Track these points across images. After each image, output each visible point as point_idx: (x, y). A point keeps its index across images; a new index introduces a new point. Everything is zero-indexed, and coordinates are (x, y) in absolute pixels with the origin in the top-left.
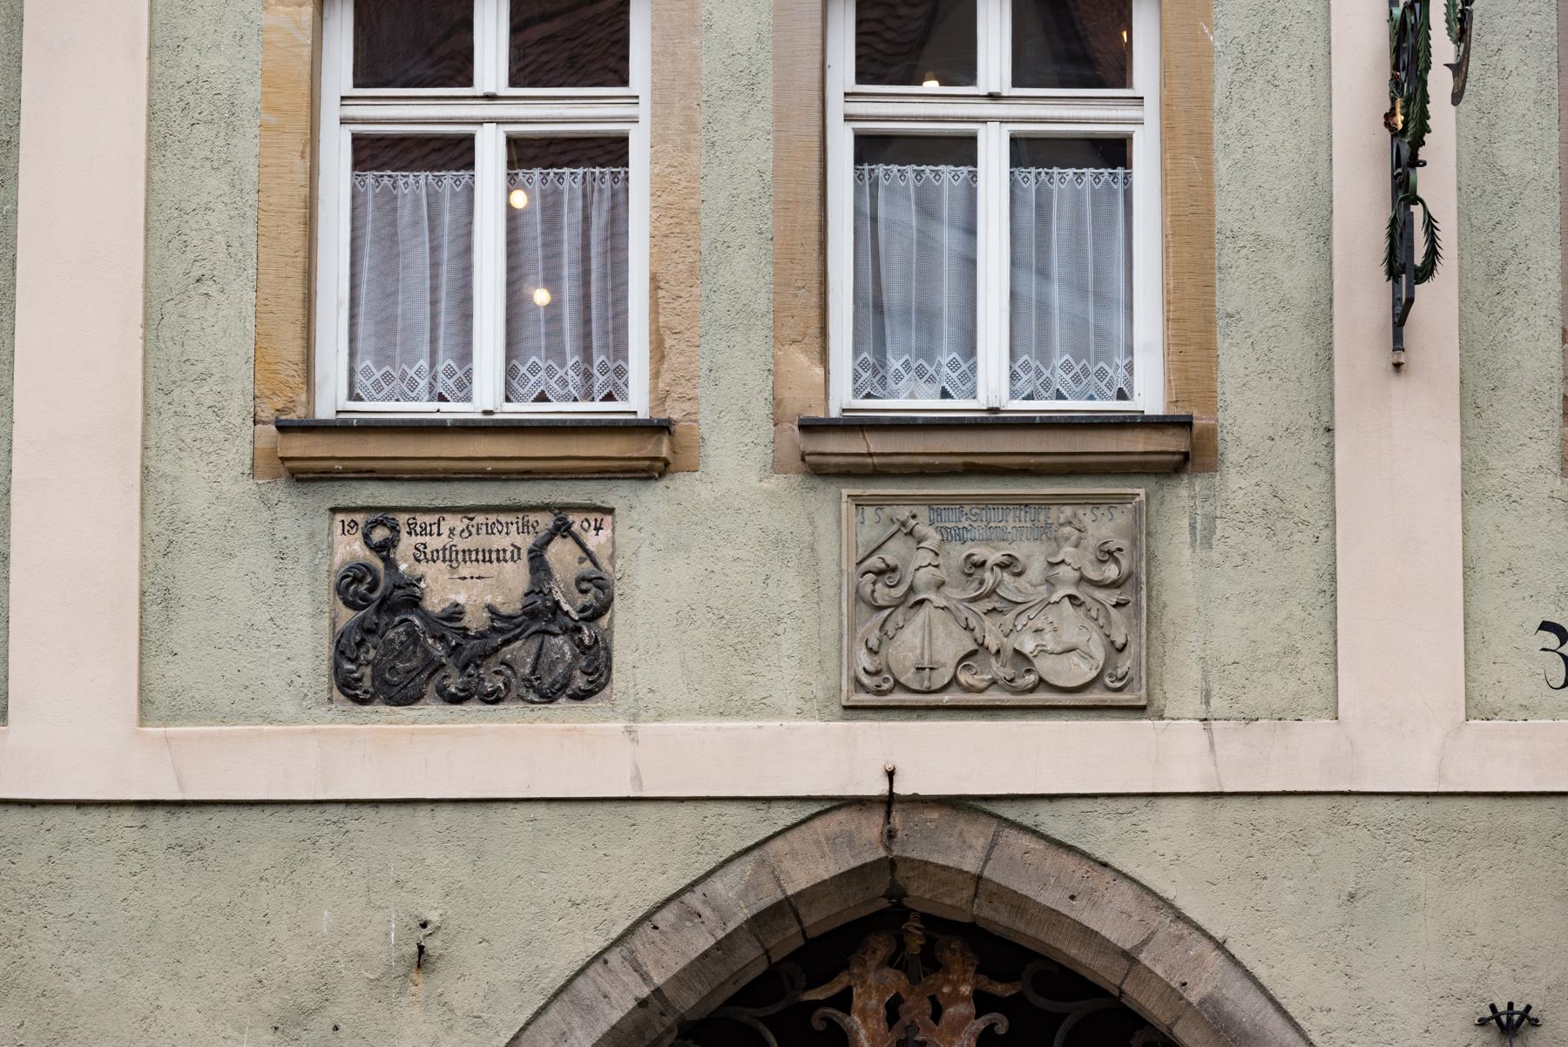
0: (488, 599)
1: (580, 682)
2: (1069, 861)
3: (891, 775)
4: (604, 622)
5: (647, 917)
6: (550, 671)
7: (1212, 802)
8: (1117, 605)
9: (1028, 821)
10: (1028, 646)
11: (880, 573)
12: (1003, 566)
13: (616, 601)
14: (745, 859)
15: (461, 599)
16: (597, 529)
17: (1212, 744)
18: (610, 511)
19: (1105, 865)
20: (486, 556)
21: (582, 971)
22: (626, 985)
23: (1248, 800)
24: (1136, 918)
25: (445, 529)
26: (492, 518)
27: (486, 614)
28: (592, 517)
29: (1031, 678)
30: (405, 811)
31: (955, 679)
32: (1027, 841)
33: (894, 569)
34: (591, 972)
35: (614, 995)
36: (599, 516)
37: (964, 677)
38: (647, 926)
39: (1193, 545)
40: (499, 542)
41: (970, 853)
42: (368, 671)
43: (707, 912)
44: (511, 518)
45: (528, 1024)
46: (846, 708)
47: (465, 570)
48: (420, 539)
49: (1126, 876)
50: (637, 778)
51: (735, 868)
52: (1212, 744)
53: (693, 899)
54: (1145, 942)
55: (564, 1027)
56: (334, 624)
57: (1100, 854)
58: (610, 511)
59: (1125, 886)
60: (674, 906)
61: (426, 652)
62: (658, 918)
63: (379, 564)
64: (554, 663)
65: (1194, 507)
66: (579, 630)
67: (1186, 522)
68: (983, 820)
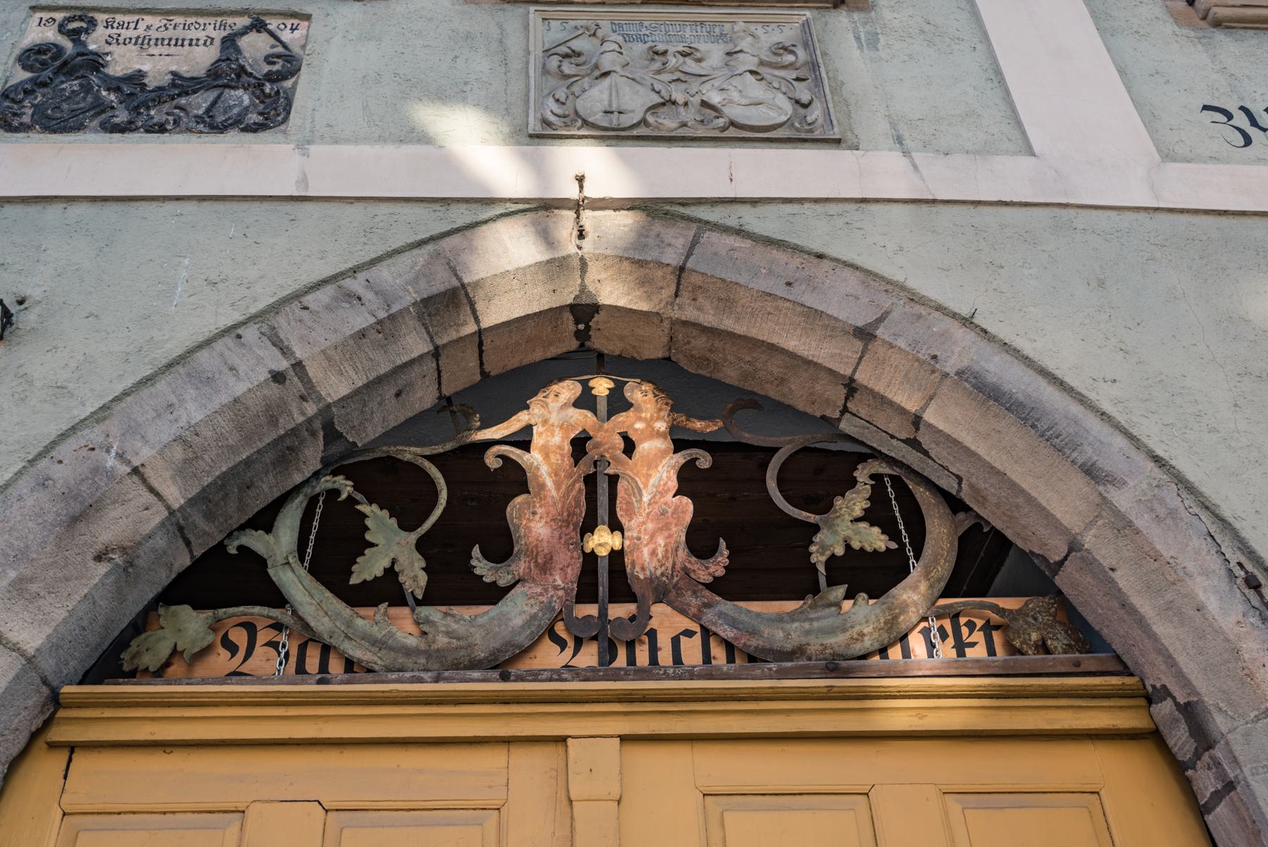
0: (174, 68)
1: (254, 118)
2: (780, 256)
3: (580, 180)
4: (288, 84)
5: (296, 296)
6: (225, 112)
7: (925, 208)
8: (798, 79)
9: (732, 222)
10: (715, 99)
11: (566, 56)
12: (684, 55)
13: (304, 69)
14: (416, 252)
15: (145, 68)
16: (293, 30)
17: (915, 167)
18: (307, 17)
19: (820, 256)
20: (180, 43)
21: (208, 343)
22: (260, 360)
23: (963, 208)
24: (865, 300)
25: (142, 26)
26: (191, 20)
27: (170, 77)
28: (289, 22)
29: (721, 122)
30: (33, 210)
31: (644, 122)
32: (731, 241)
33: (579, 54)
34: (219, 346)
35: (242, 369)
36: (296, 22)
37: (651, 119)
38: (296, 306)
39: (860, 47)
40: (192, 34)
41: (669, 250)
42: (30, 112)
43: (368, 296)
44: (212, 20)
45: (126, 393)
46: (531, 136)
47: (153, 50)
48: (115, 31)
49: (847, 264)
50: (304, 180)
51: (406, 259)
52: (915, 167)
53: (355, 285)
54: (880, 320)
55: (173, 399)
56: (6, 82)
57: (816, 246)
58: (307, 17)
59: (847, 272)
60: (330, 290)
61: (97, 97)
62: (309, 299)
63: (68, 45)
64: (230, 108)
65: (856, 27)
66: (260, 86)
67: (851, 36)
68: (682, 224)
